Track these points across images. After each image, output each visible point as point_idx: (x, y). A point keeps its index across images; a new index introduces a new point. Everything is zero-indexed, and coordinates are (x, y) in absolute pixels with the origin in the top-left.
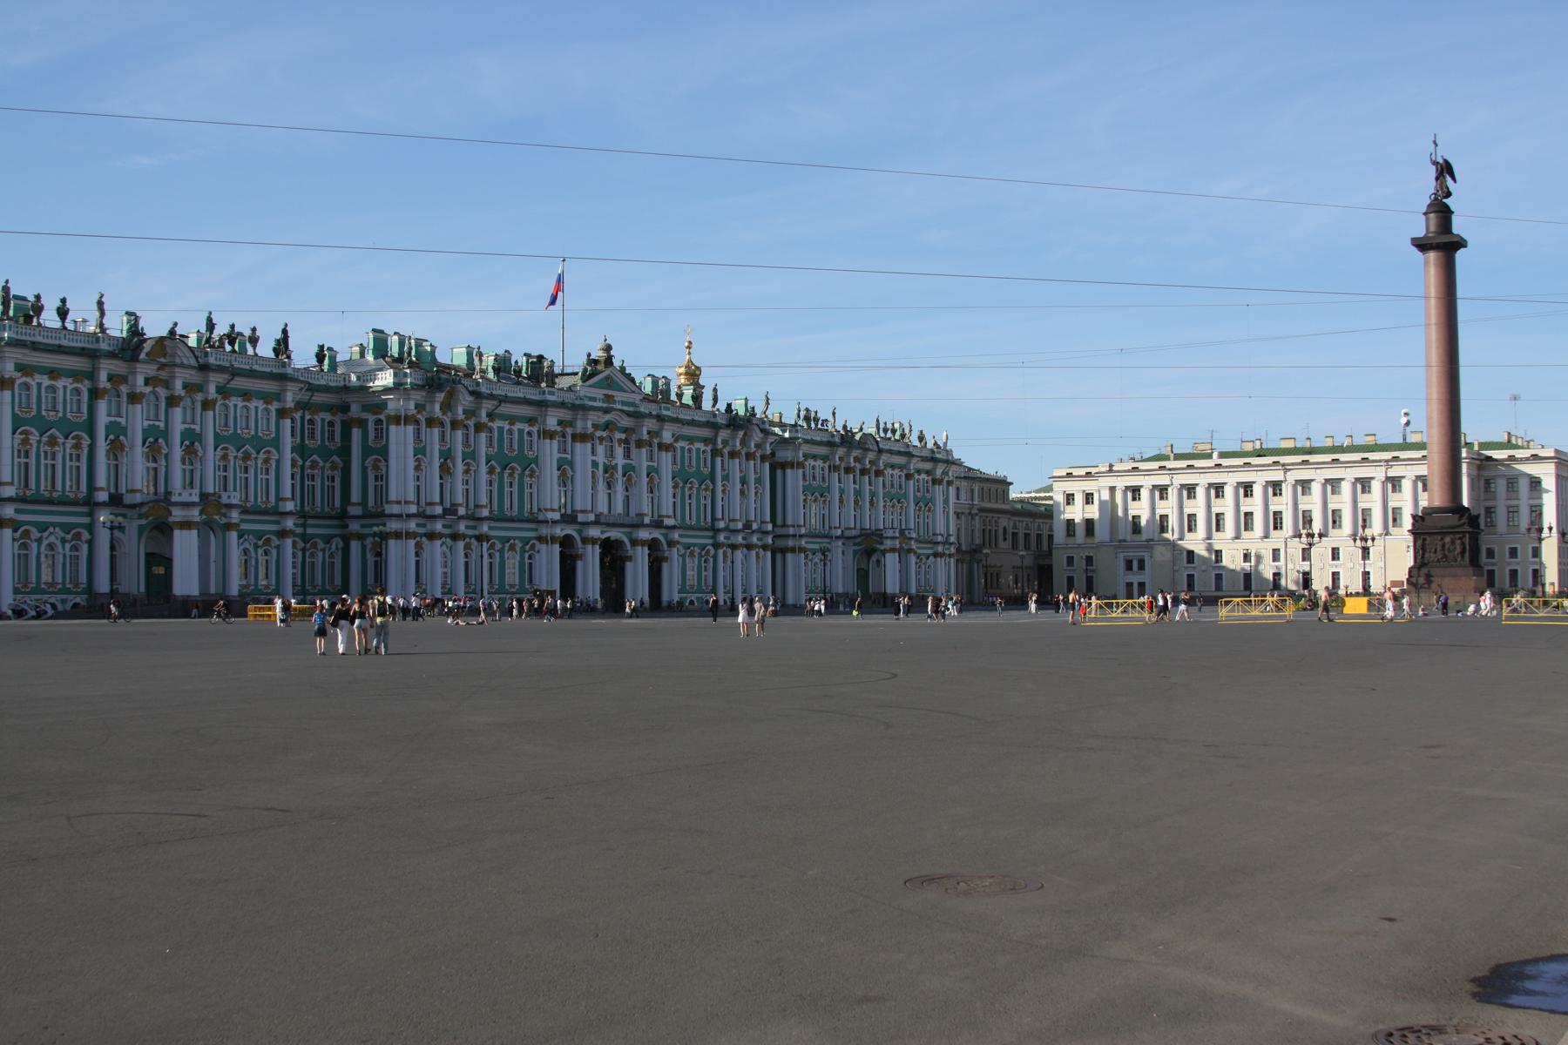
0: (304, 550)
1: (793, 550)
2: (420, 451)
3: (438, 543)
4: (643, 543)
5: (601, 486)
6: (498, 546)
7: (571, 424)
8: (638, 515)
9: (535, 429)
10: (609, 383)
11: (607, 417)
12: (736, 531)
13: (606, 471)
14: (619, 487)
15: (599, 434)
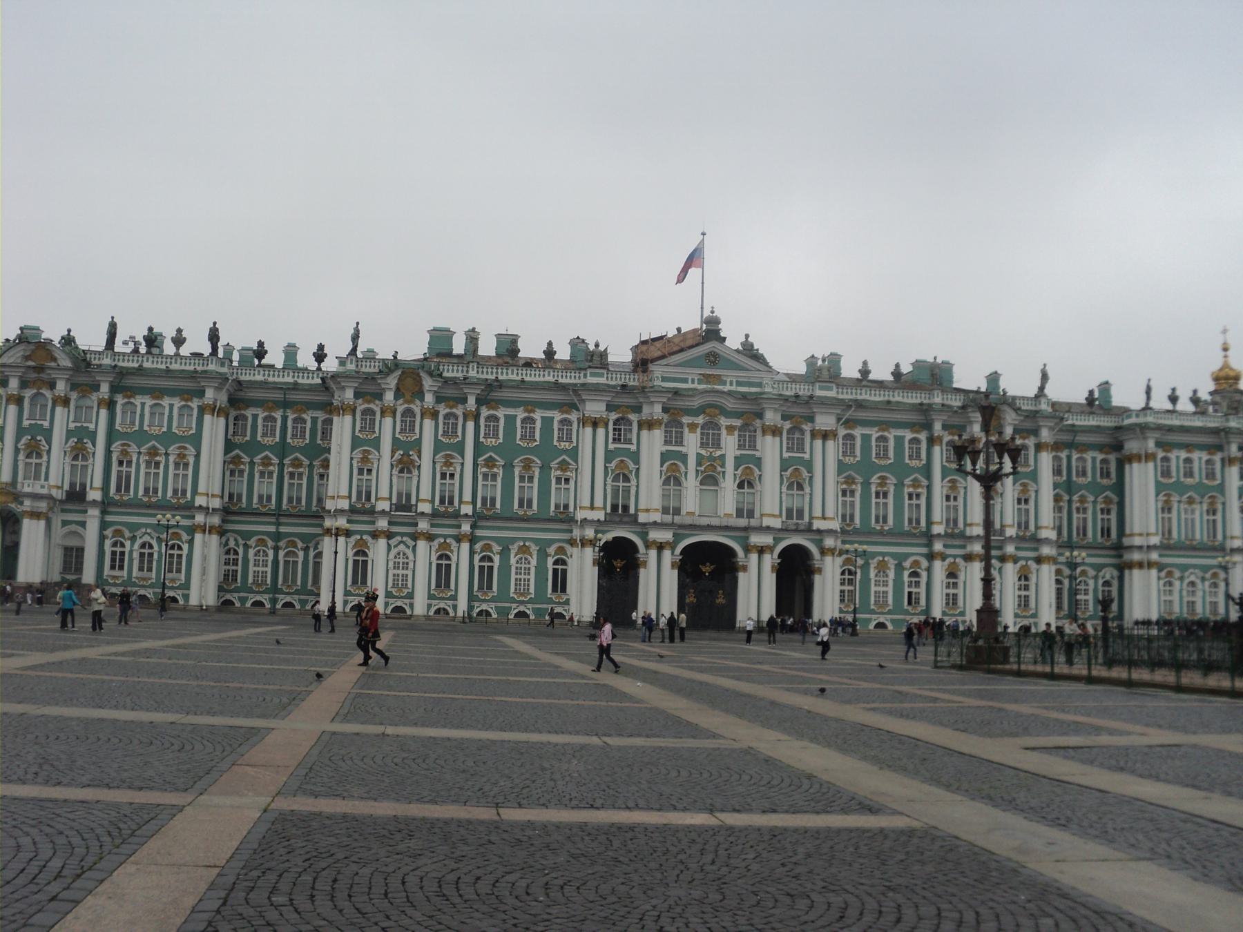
0: (276, 549)
1: (1140, 565)
2: (364, 444)
3: (382, 542)
4: (761, 551)
5: (691, 483)
6: (496, 548)
7: (638, 409)
8: (762, 515)
9: (573, 416)
10: (713, 359)
11: (696, 403)
12: (971, 539)
13: (699, 464)
14: (729, 484)
15: (686, 420)
